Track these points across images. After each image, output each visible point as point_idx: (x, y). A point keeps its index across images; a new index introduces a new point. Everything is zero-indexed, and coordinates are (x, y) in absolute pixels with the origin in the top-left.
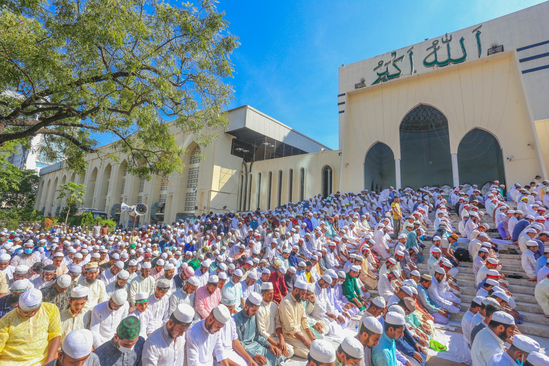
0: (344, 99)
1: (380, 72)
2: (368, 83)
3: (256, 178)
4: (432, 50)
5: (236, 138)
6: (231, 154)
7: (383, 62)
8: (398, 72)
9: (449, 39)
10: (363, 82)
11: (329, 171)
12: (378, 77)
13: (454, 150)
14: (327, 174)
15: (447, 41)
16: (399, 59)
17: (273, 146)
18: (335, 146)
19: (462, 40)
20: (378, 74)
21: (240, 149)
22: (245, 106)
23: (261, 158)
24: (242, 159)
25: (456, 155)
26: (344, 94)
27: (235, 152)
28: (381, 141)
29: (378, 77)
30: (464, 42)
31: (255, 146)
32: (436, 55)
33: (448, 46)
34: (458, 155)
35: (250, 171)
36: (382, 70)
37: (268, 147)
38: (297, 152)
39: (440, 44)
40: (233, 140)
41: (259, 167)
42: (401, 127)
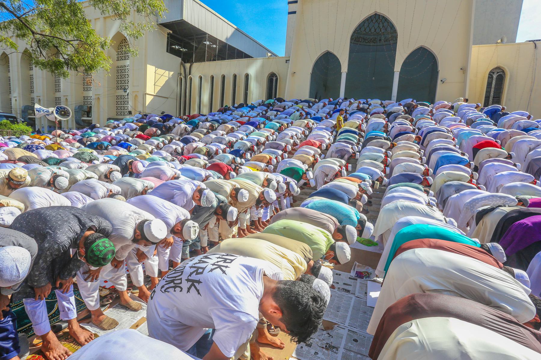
3: (196, 81)
5: (171, 32)
6: (167, 51)
11: (274, 79)
14: (272, 82)
17: (214, 46)
21: (177, 47)
23: (201, 59)
24: (179, 60)
25: (399, 73)
28: (331, 50)
31: (194, 44)
35: (190, 74)
37: (209, 46)
38: (241, 55)
40: (168, 34)
41: (200, 70)
42: (352, 39)
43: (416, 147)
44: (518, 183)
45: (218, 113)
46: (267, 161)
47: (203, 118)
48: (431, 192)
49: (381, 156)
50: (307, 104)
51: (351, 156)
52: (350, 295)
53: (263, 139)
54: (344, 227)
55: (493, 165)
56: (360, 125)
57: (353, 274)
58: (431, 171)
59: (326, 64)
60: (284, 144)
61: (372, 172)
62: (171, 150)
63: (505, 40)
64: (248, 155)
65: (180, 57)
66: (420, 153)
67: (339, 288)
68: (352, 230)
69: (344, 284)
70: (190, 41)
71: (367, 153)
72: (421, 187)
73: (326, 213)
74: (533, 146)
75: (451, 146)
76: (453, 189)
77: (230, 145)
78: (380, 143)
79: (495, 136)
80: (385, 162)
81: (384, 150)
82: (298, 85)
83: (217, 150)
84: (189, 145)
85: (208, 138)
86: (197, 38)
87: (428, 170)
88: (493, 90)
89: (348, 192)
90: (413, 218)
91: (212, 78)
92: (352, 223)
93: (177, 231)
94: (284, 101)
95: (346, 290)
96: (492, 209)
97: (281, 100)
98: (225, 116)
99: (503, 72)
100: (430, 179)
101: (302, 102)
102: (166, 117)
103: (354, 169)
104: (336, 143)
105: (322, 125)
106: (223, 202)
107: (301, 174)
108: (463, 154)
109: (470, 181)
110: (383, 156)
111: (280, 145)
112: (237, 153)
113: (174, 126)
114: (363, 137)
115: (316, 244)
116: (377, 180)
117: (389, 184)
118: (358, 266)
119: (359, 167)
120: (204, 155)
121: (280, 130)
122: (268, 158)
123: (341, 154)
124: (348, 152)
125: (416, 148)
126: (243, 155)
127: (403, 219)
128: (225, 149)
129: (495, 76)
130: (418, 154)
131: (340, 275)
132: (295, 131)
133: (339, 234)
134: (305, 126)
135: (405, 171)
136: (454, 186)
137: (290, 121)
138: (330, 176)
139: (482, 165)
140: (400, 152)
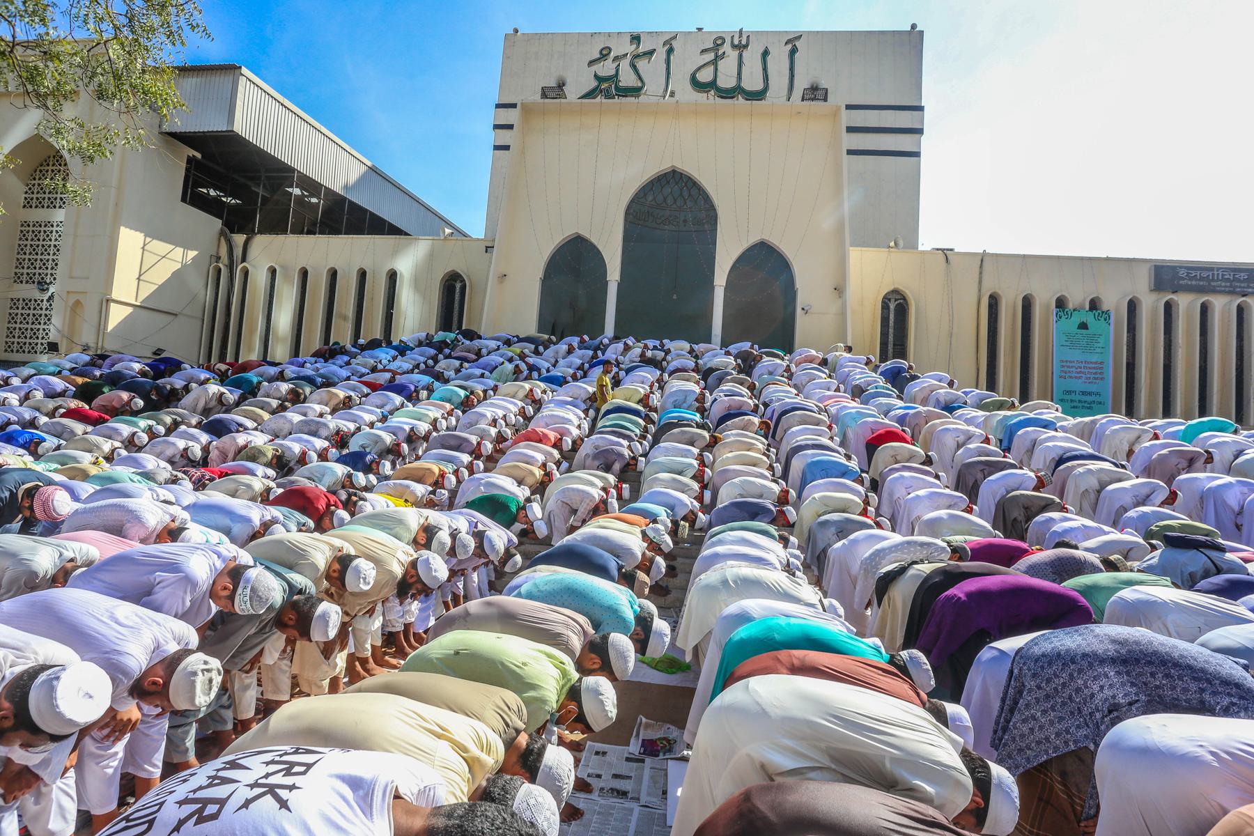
0: (511, 116)
1: (600, 74)
3: (259, 279)
4: (711, 56)
5: (199, 156)
6: (184, 200)
7: (610, 49)
9: (744, 42)
10: (561, 85)
11: (458, 285)
12: (594, 84)
13: (720, 279)
14: (453, 295)
16: (645, 54)
17: (314, 200)
18: (476, 227)
19: (766, 53)
20: (596, 76)
21: (212, 193)
22: (231, 69)
23: (276, 226)
24: (217, 223)
26: (514, 106)
27: (192, 197)
28: (585, 233)
29: (594, 84)
30: (769, 58)
31: (261, 191)
32: (716, 70)
33: (740, 56)
34: (728, 288)
35: (244, 260)
36: (606, 68)
37: (299, 200)
38: (379, 226)
39: (727, 48)
40: (190, 160)
41: (268, 252)
43: (760, 443)
44: (943, 513)
45: (313, 359)
46: (432, 480)
47: (272, 371)
48: (793, 539)
49: (691, 465)
50: (533, 347)
51: (628, 464)
52: (628, 804)
53: (423, 427)
54: (605, 638)
55: (902, 477)
56: (647, 396)
57: (634, 747)
58: (793, 493)
59: (573, 262)
60: (474, 439)
61: (672, 502)
62: (169, 452)
63: (901, 243)
64: (386, 467)
65: (219, 216)
66: (768, 456)
67: (602, 789)
68: (622, 642)
69: (616, 776)
70: (249, 183)
71: (662, 459)
72: (772, 529)
73: (563, 606)
74: (961, 439)
75: (825, 441)
76: (833, 530)
77: (340, 440)
78: (687, 436)
79: (901, 420)
80: (698, 477)
81: (696, 451)
82: (512, 302)
83: (304, 453)
84: (225, 439)
85: (282, 421)
86: (268, 178)
87: (787, 492)
88: (891, 331)
89: (618, 551)
90: (753, 605)
91: (304, 274)
92: (621, 625)
93: (153, 688)
94: (480, 337)
95: (618, 792)
96: (902, 570)
97: (471, 335)
98: (333, 368)
99: (904, 299)
100: (789, 509)
101: (520, 340)
102: (164, 365)
103: (636, 494)
104: (593, 437)
105: (563, 394)
106: (300, 592)
107: (514, 509)
108: (848, 458)
109: (864, 513)
110: (695, 463)
111: (466, 440)
112: (356, 461)
113: (187, 389)
114: (654, 423)
115: (533, 687)
116: (684, 518)
117: (710, 526)
118: (647, 726)
119: (646, 491)
120: (268, 465)
121: (466, 405)
122: (437, 471)
123: (605, 461)
124: (621, 455)
125: (761, 446)
126: (374, 466)
127: (733, 608)
128: (326, 450)
129: (892, 306)
130: (765, 459)
131: (604, 753)
132: (501, 408)
133: (593, 656)
134: (526, 396)
135: (742, 496)
136: (835, 523)
137: (491, 383)
138: (582, 512)
139: (884, 476)
140: (730, 455)
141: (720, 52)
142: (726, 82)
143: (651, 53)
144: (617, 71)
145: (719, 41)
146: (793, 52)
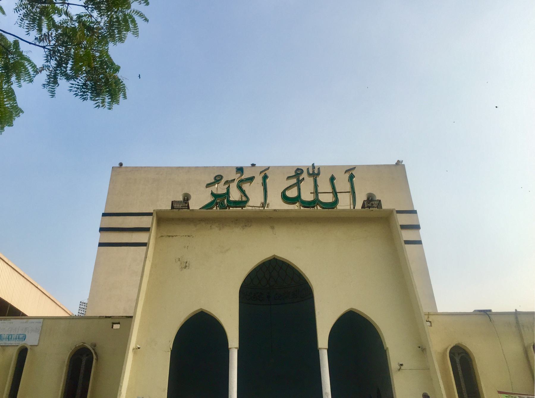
1: (215, 192)
2: (195, 204)
4: (294, 181)
8: (244, 199)
9: (316, 172)
10: (187, 198)
11: (84, 359)
15: (315, 173)
19: (332, 179)
20: (212, 194)
39: (304, 175)
129: (457, 360)
141: (301, 178)
142: (307, 196)
143: (251, 179)
144: (228, 189)
145: (299, 172)
146: (352, 177)
